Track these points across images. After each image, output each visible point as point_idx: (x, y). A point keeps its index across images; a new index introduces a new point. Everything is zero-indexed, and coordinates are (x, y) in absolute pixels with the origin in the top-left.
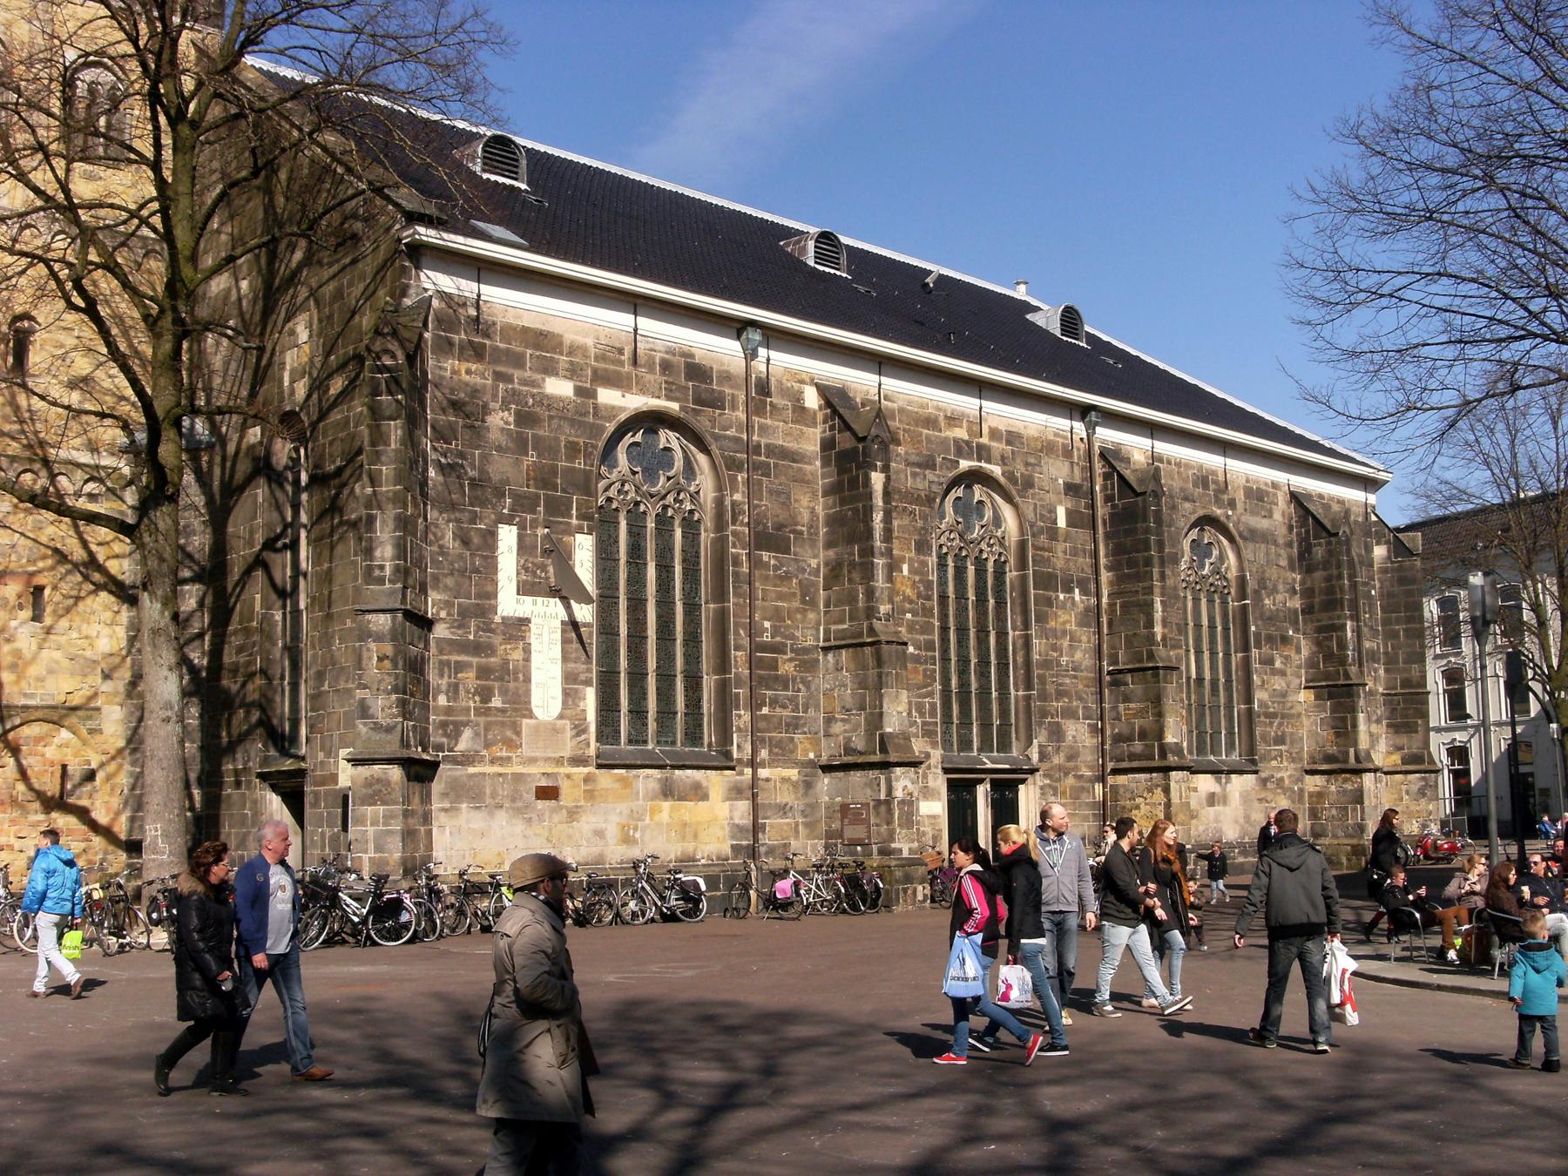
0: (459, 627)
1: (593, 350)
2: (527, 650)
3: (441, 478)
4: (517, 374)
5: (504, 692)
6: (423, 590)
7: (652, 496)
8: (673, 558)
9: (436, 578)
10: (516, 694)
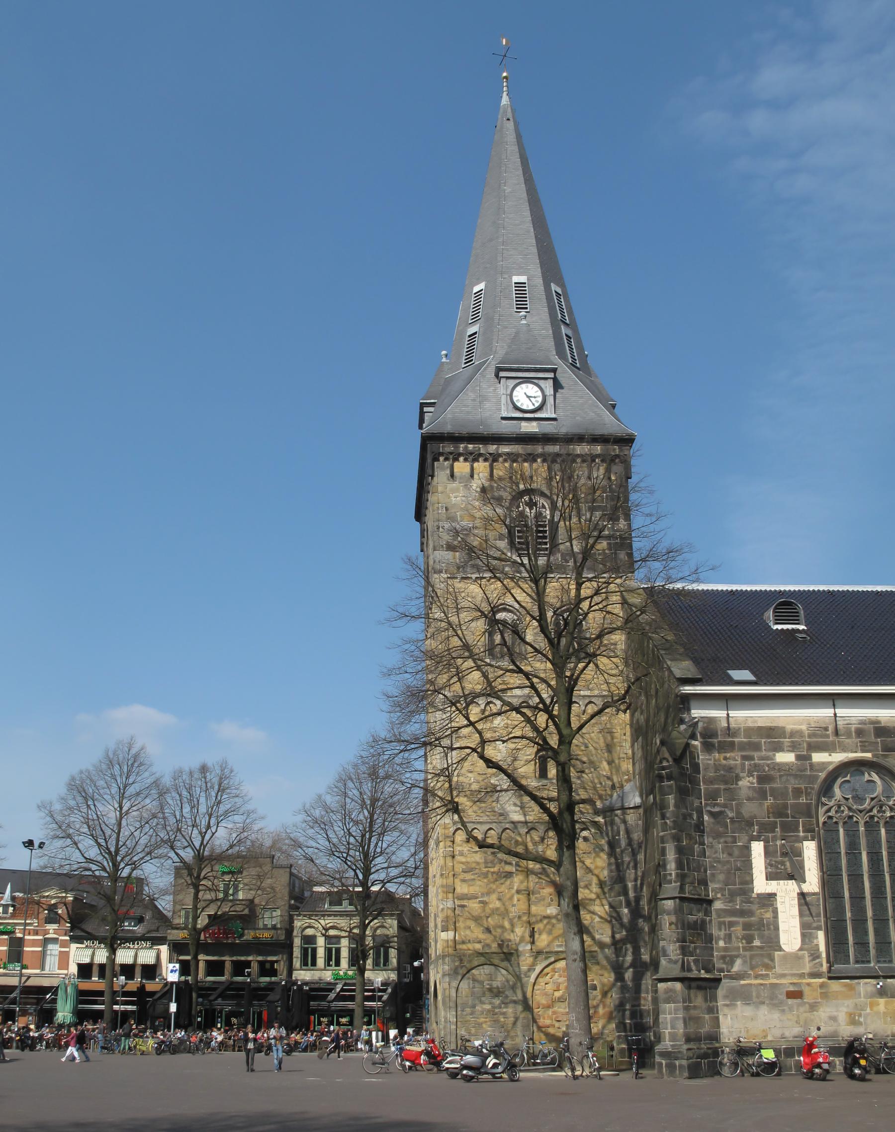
0: (729, 902)
1: (806, 733)
2: (775, 912)
3: (712, 820)
4: (756, 754)
5: (761, 937)
6: (704, 882)
7: (861, 811)
8: (880, 847)
9: (713, 875)
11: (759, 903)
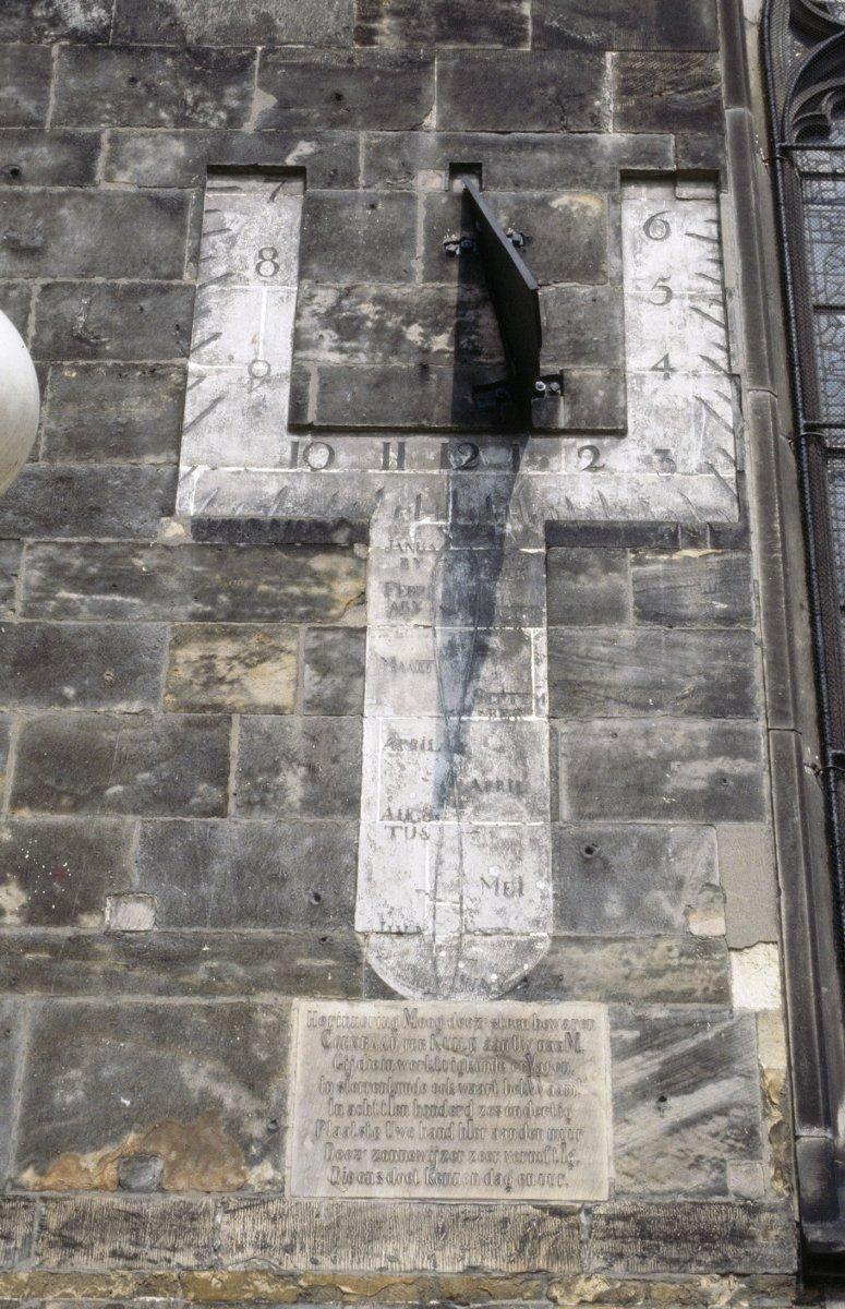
10: (258, 871)
11: (204, 593)
